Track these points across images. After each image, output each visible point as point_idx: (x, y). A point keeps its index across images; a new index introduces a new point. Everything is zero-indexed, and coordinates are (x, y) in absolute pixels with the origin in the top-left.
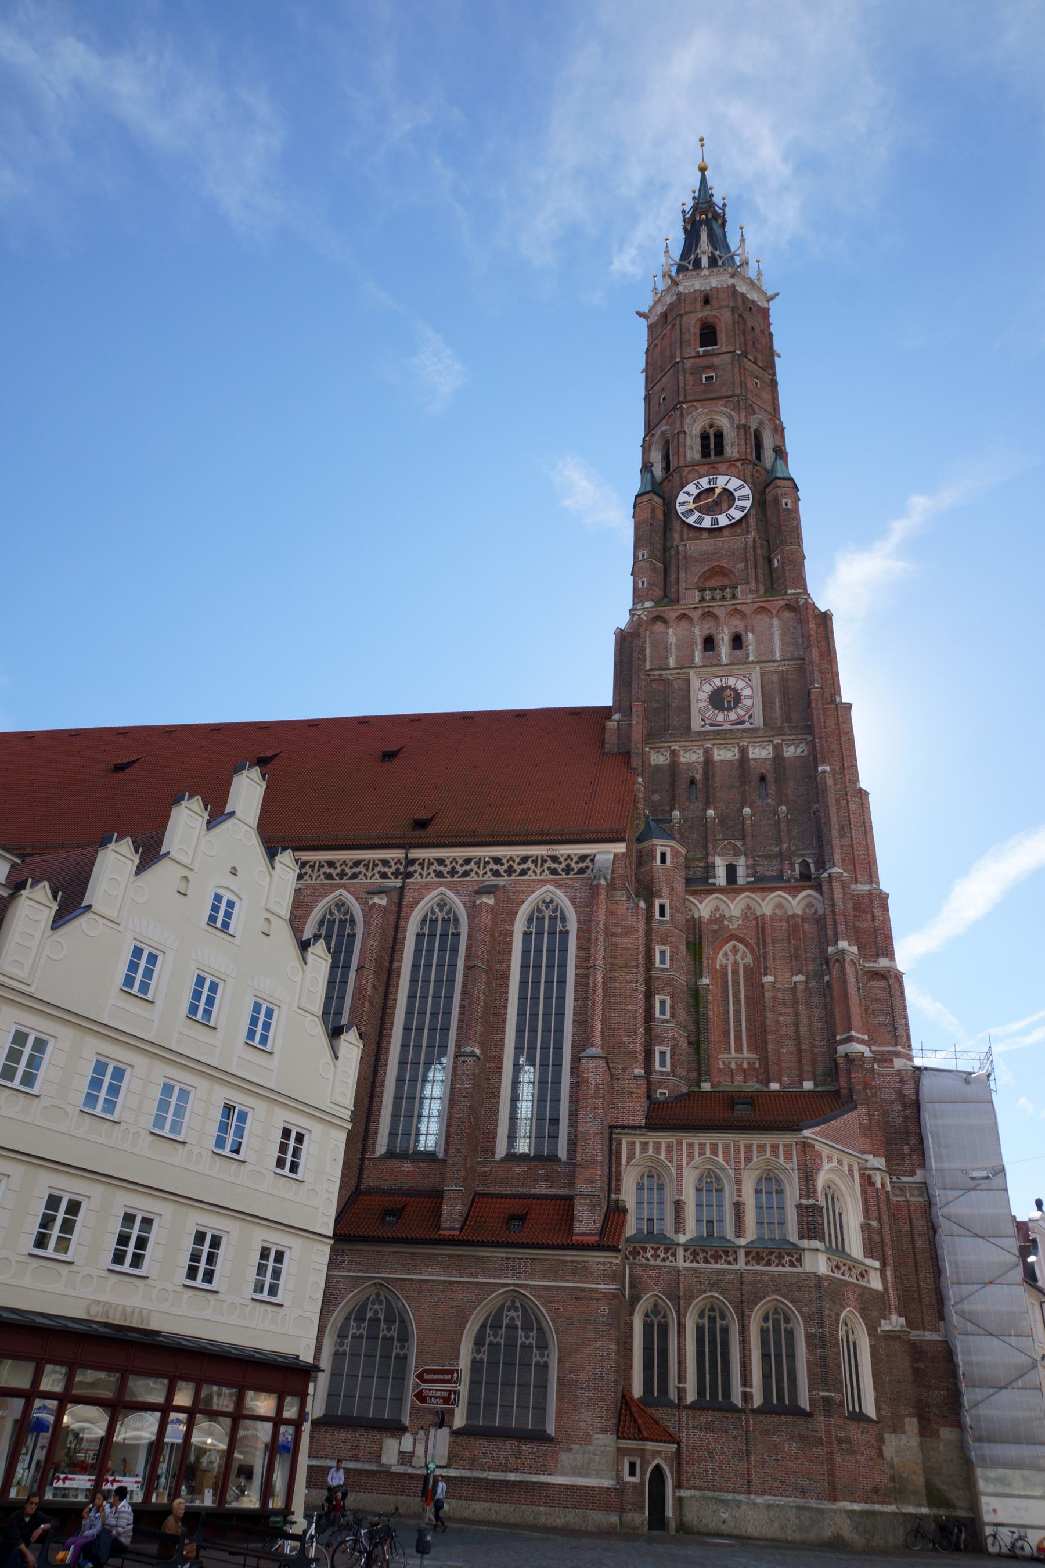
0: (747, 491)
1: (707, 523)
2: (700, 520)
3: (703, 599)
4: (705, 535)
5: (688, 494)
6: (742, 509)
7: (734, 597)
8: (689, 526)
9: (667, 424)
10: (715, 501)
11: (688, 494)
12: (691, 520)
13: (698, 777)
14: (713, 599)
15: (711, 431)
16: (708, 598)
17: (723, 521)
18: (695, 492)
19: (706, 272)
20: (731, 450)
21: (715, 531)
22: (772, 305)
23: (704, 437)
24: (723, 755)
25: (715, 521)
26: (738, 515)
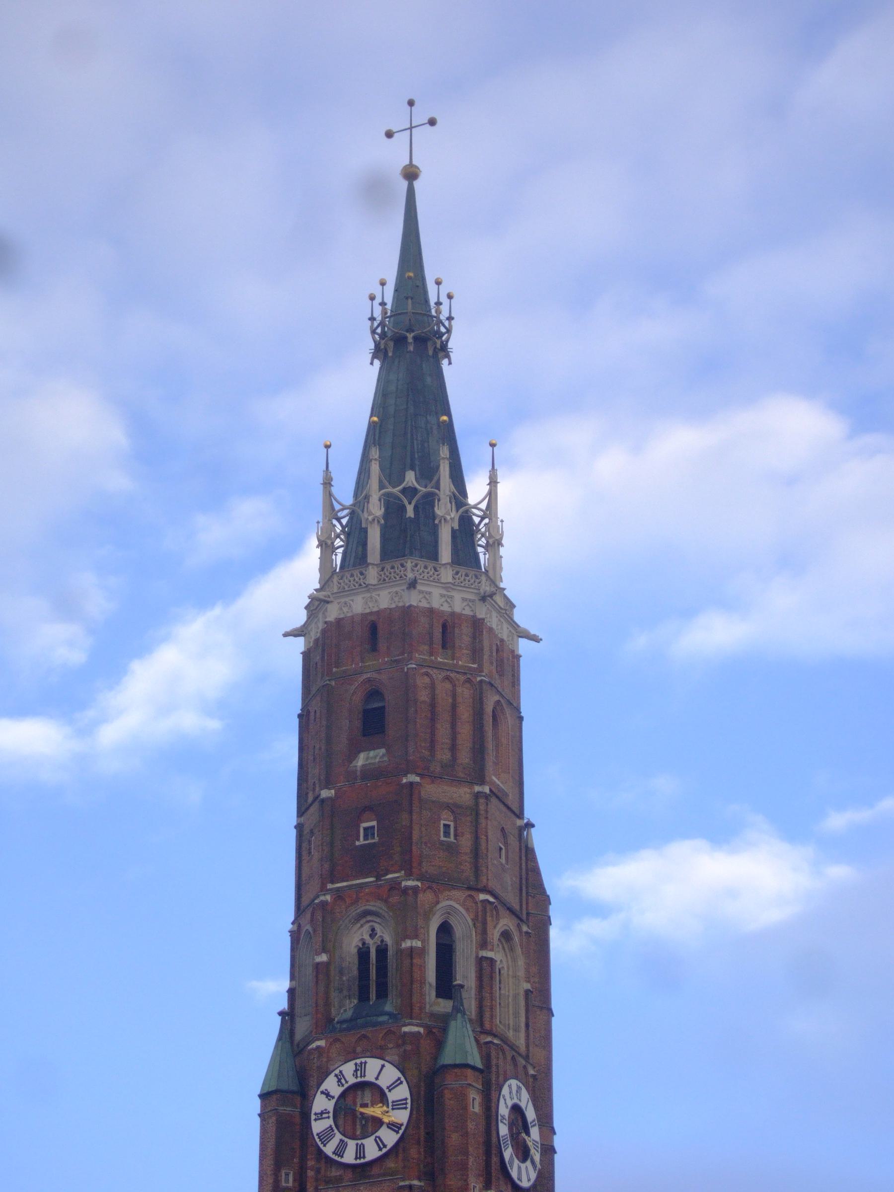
0: (403, 1092)
1: (349, 1157)
4: (349, 1174)
5: (327, 1094)
6: (394, 1126)
8: (327, 1157)
11: (327, 1094)
12: (329, 1150)
19: (372, 575)
21: (362, 1170)
25: (360, 1152)
26: (390, 1138)
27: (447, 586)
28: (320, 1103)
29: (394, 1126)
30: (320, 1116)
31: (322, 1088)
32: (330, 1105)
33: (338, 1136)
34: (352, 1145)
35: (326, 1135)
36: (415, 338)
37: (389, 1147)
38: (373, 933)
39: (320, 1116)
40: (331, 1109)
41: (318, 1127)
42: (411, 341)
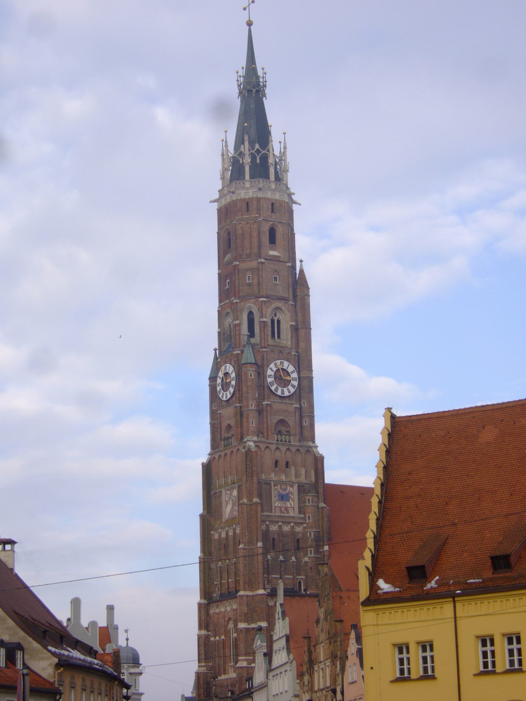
0: (295, 375)
1: (279, 393)
2: (276, 390)
3: (277, 441)
5: (272, 370)
6: (293, 386)
7: (289, 442)
9: (254, 304)
10: (281, 378)
11: (272, 370)
12: (273, 388)
13: (276, 537)
14: (281, 441)
15: (276, 319)
16: (280, 439)
17: (286, 394)
18: (275, 369)
20: (286, 338)
22: (294, 205)
23: (273, 321)
24: (286, 528)
25: (283, 392)
26: (292, 390)
27: (273, 190)
28: (269, 372)
29: (293, 386)
30: (270, 376)
31: (270, 367)
32: (273, 374)
33: (276, 385)
34: (280, 389)
35: (272, 384)
36: (256, 91)
37: (292, 392)
38: (276, 316)
39: (270, 376)
40: (273, 375)
41: (270, 380)
42: (253, 90)
